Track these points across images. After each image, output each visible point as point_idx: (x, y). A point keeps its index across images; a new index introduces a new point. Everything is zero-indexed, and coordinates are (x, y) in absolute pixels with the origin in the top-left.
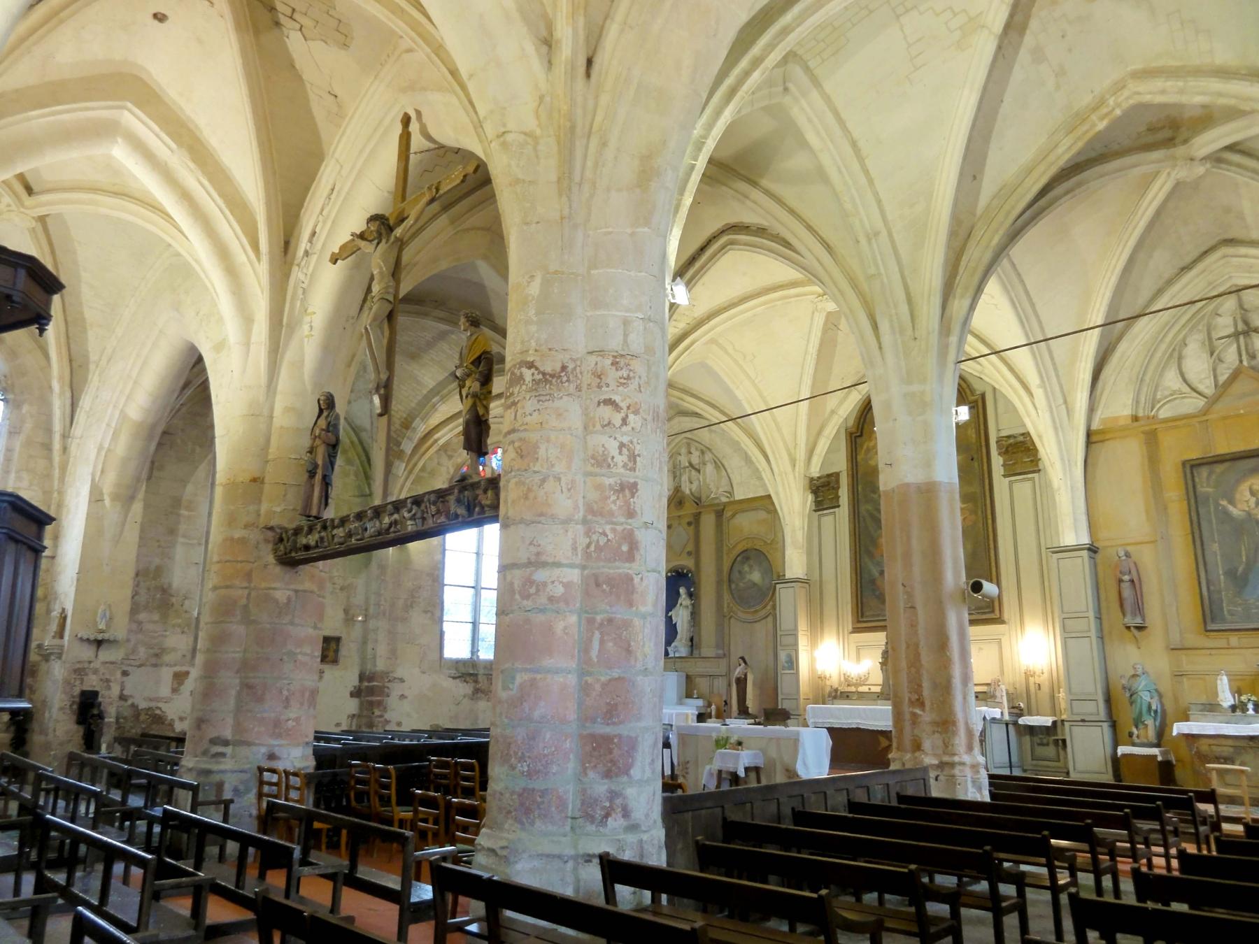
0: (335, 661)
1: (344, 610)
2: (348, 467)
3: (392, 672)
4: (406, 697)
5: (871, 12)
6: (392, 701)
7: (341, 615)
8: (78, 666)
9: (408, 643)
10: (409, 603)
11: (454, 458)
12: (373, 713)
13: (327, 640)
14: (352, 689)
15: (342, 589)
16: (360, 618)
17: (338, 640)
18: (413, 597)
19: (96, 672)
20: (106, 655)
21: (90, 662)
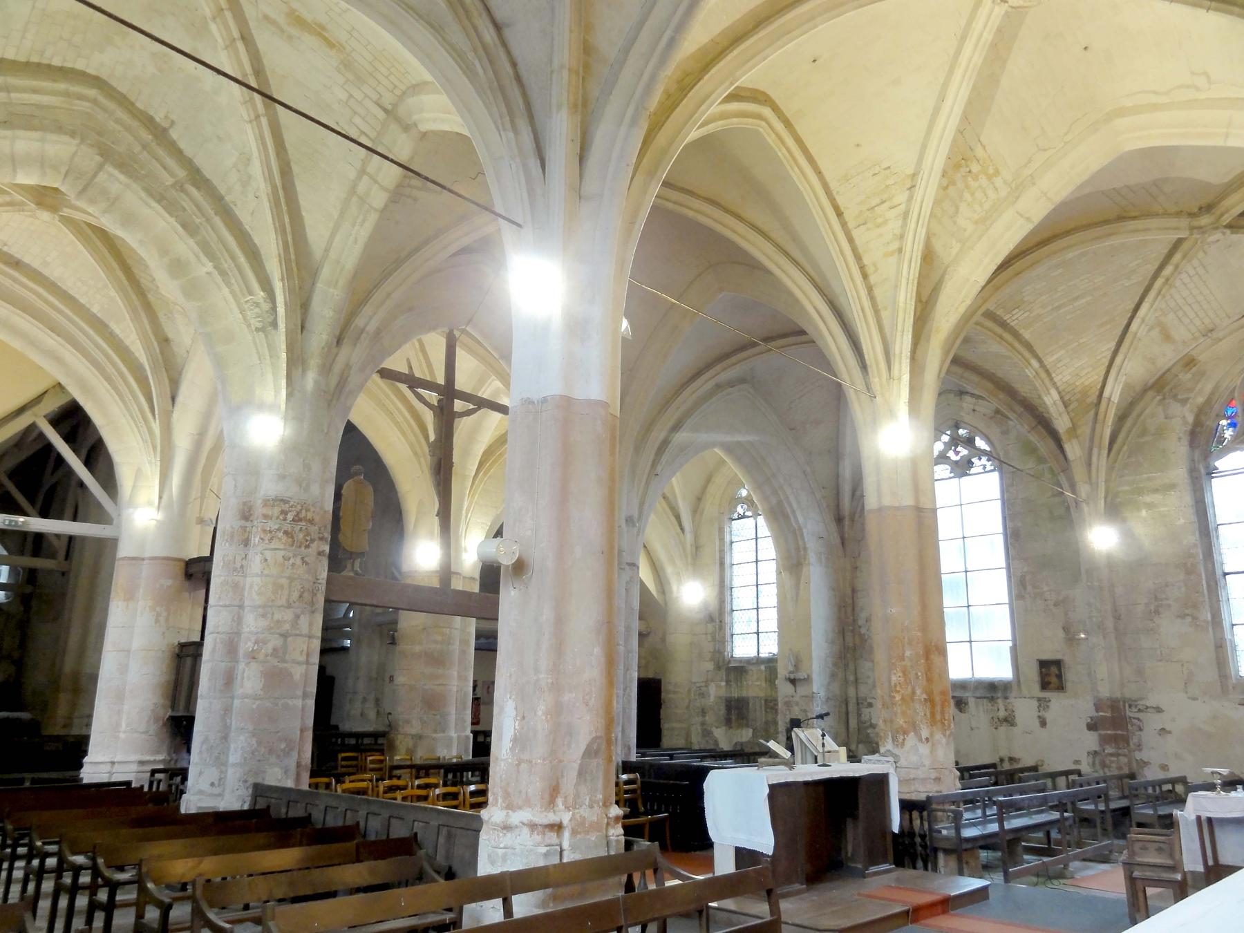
0: (1061, 688)
1: (1063, 628)
2: (1041, 467)
3: (1142, 699)
4: (1170, 732)
5: (354, 28)
6: (1149, 735)
7: (1061, 634)
8: (787, 699)
9: (1160, 661)
10: (1152, 608)
11: (1191, 400)
12: (1104, 751)
13: (1043, 664)
14: (1089, 720)
15: (1055, 605)
16: (1083, 636)
17: (1058, 663)
18: (1156, 598)
19: (797, 704)
20: (802, 690)
21: (793, 697)
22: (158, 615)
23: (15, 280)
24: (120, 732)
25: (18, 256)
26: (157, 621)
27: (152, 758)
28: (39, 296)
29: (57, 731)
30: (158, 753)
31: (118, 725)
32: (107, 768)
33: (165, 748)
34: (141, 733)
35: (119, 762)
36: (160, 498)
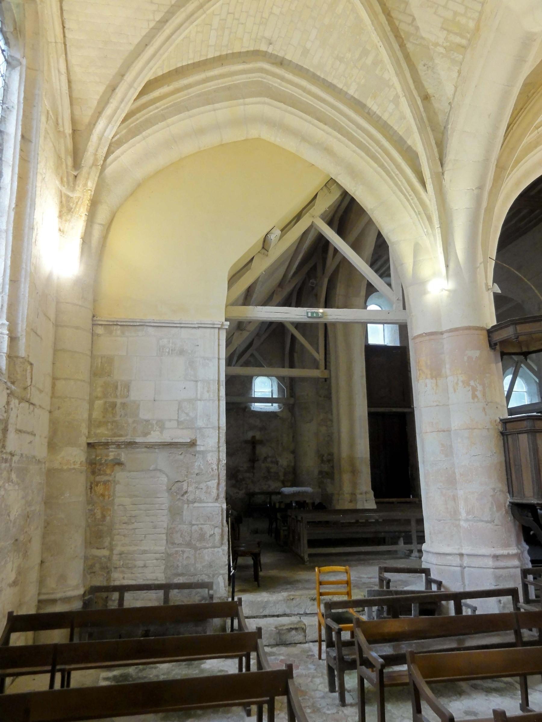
22: (474, 390)
23: (283, 79)
24: (459, 520)
25: (281, 54)
26: (474, 396)
27: (505, 552)
28: (304, 90)
29: (347, 506)
30: (507, 545)
31: (455, 513)
32: (457, 561)
33: (513, 539)
34: (487, 522)
35: (468, 555)
36: (447, 266)
